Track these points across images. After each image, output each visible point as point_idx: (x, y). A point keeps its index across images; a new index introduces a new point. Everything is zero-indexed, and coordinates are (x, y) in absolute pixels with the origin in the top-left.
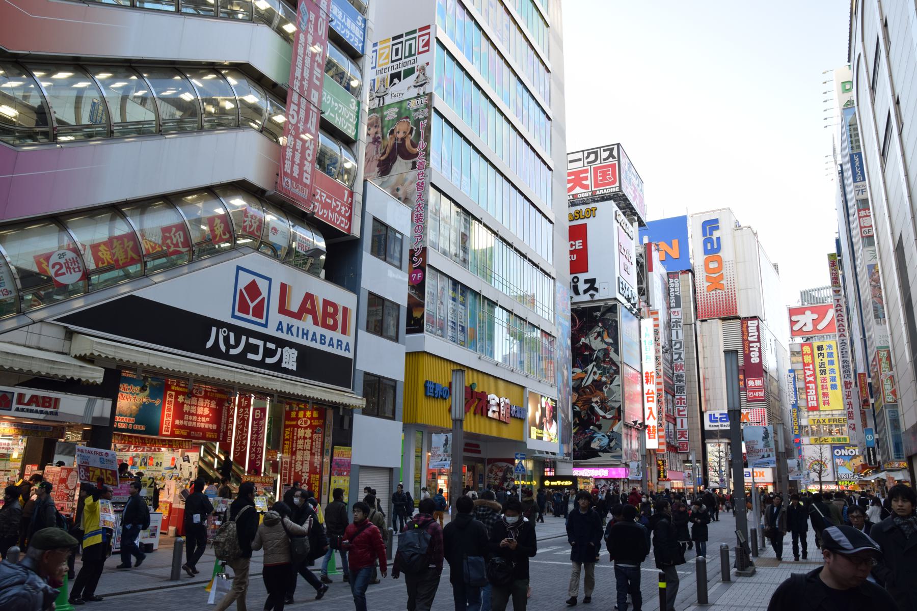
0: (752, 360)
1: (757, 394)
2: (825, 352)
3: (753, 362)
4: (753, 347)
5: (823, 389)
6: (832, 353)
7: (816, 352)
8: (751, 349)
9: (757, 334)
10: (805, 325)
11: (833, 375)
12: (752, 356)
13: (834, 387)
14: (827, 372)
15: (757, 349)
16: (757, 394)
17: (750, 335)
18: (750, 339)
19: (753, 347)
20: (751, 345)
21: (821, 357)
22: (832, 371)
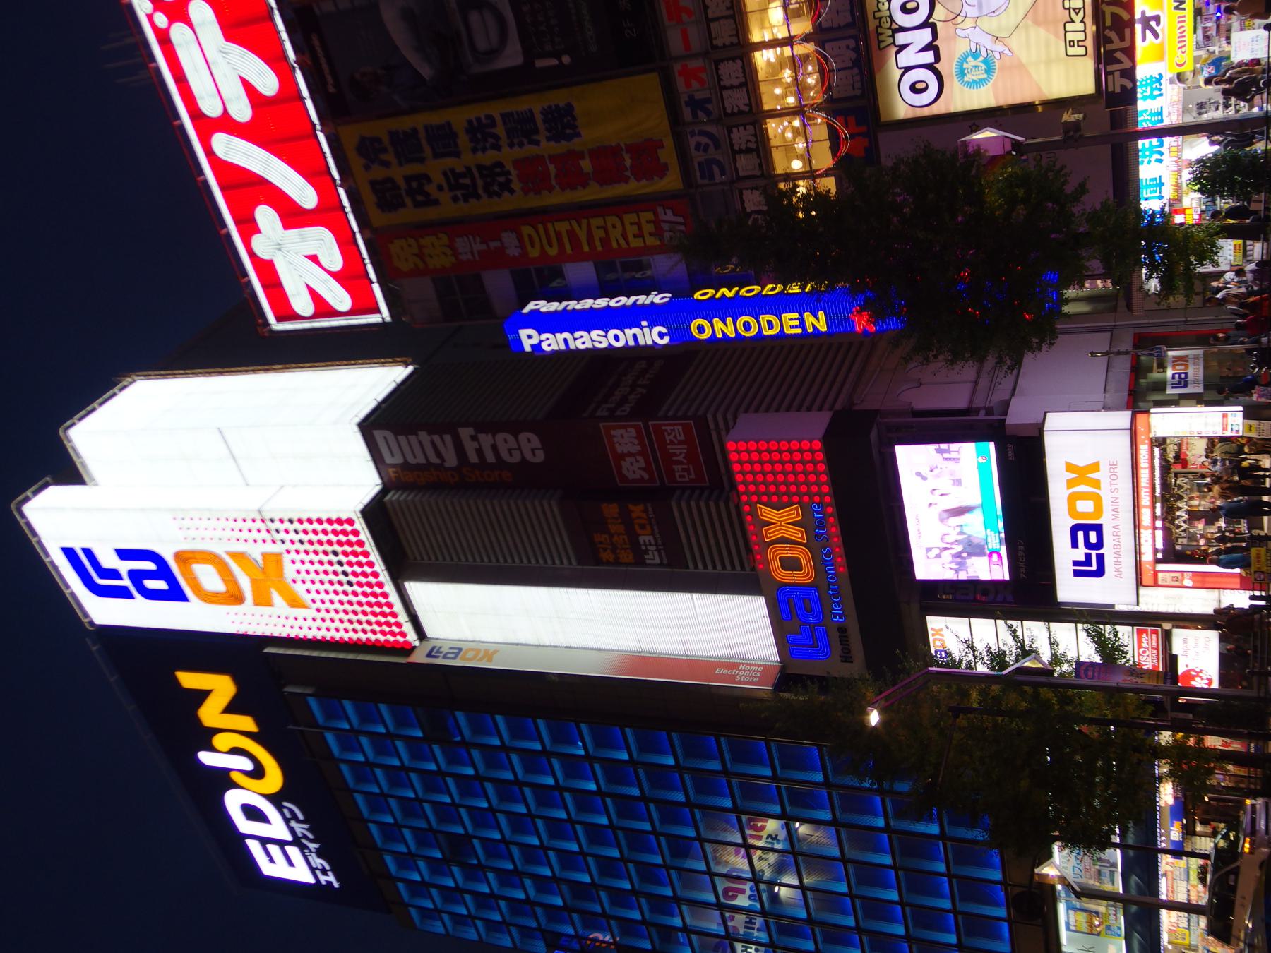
0: (529, 456)
1: (679, 451)
3: (540, 457)
4: (479, 452)
7: (409, 214)
8: (490, 458)
9: (423, 435)
10: (314, 259)
11: (500, 130)
12: (516, 458)
14: (488, 157)
15: (486, 440)
16: (679, 451)
17: (434, 459)
18: (451, 460)
19: (479, 452)
20: (474, 458)
21: (431, 189)
22: (480, 133)
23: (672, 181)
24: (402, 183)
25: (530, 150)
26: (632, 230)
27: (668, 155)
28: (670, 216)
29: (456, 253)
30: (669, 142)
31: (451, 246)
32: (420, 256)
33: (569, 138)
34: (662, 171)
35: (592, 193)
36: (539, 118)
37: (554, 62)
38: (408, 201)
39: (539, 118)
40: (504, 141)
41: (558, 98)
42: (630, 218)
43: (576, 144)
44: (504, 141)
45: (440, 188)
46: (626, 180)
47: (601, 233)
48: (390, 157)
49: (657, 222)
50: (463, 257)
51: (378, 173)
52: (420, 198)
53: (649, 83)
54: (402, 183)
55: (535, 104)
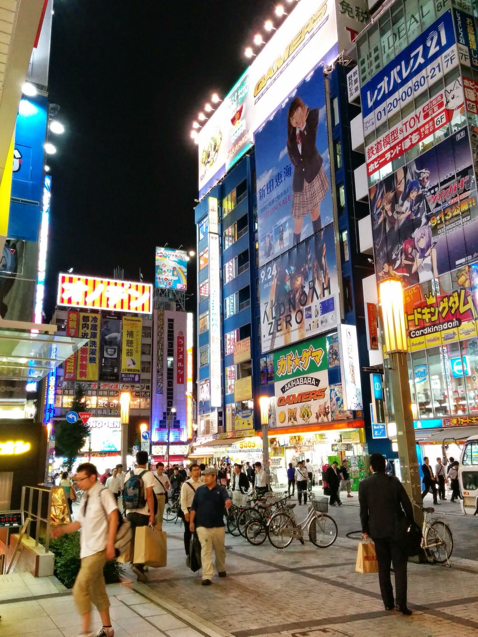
2: (90, 323)
5: (82, 361)
6: (96, 325)
7: (81, 322)
11: (93, 348)
13: (92, 360)
21: (85, 329)
23: (78, 378)
24: (88, 323)
25: (89, 352)
26: (70, 367)
27: (83, 378)
28: (72, 376)
29: (72, 328)
30: (85, 379)
31: (73, 328)
32: (72, 320)
33: (90, 360)
34: (81, 376)
35: (79, 362)
36: (94, 356)
37: (103, 362)
38: (84, 323)
39: (94, 356)
40: (91, 348)
41: (97, 361)
42: (73, 368)
43: (88, 361)
44: (91, 348)
45: (85, 331)
46: (80, 369)
47: (71, 361)
48: (93, 323)
49: (71, 373)
50: (70, 330)
51: (90, 319)
52: (84, 326)
53: (96, 378)
54: (88, 323)
55: (97, 356)
